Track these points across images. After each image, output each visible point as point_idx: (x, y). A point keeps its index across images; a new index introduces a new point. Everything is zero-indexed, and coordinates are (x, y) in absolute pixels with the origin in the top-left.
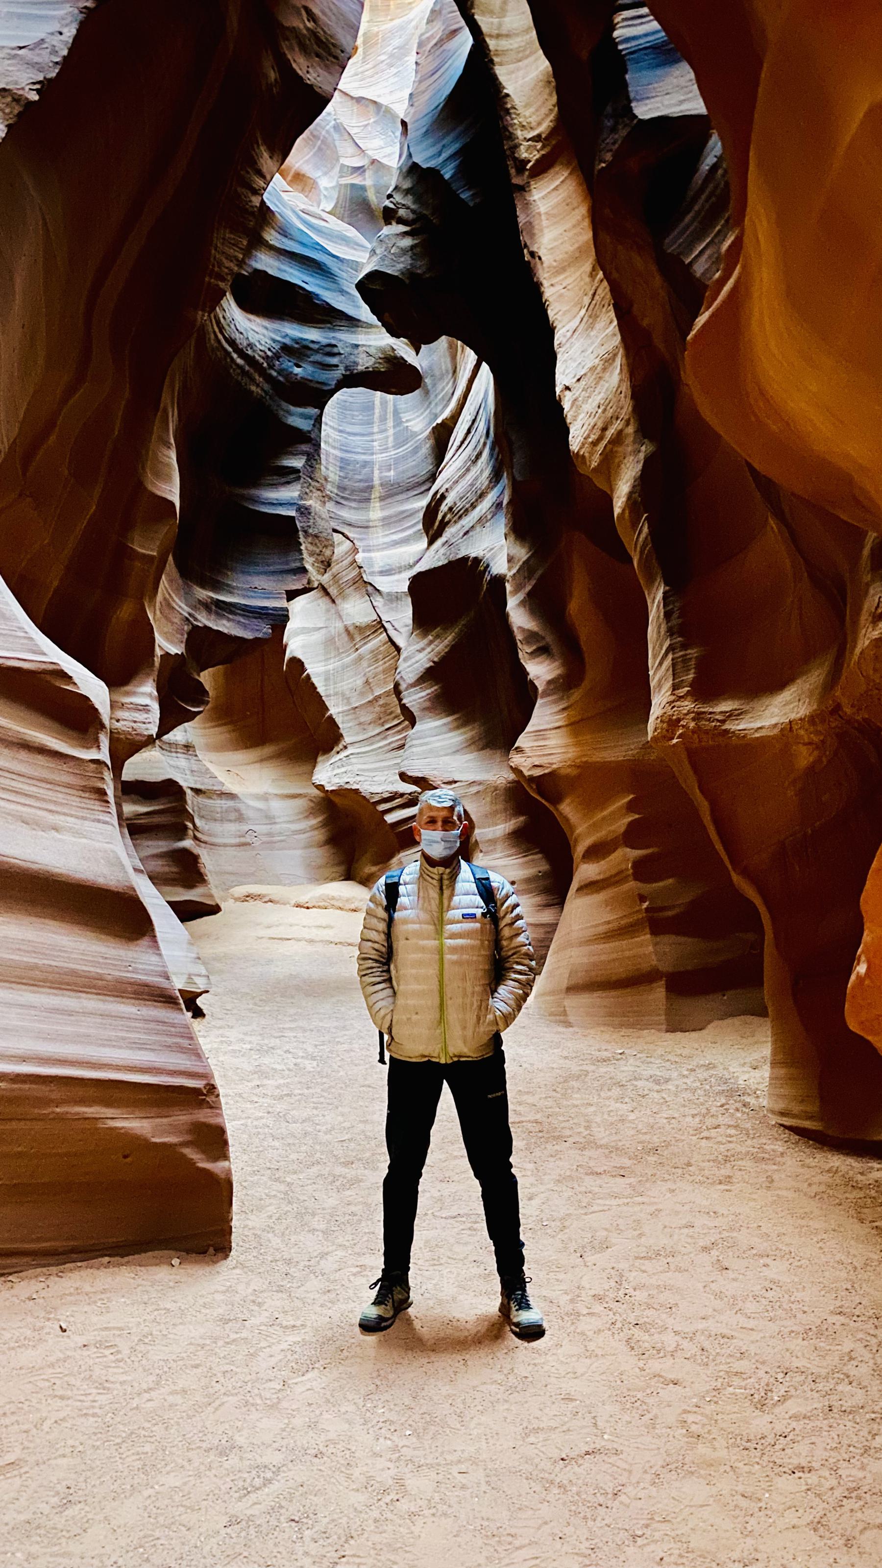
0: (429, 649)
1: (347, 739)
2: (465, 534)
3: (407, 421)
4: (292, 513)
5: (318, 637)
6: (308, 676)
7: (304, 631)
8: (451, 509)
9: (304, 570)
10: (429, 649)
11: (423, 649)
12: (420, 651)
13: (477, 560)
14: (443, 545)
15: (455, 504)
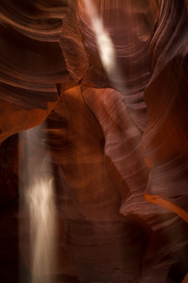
0: (156, 125)
1: (132, 190)
2: (167, 53)
3: (141, 39)
4: (58, 41)
5: (116, 147)
6: (113, 164)
7: (111, 145)
8: (158, 47)
9: (68, 72)
10: (156, 125)
11: (153, 126)
12: (152, 128)
13: (174, 59)
14: (157, 67)
15: (160, 42)
